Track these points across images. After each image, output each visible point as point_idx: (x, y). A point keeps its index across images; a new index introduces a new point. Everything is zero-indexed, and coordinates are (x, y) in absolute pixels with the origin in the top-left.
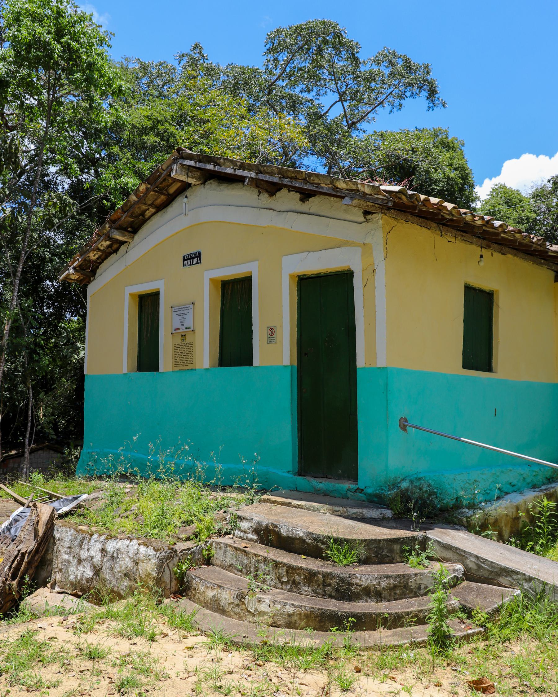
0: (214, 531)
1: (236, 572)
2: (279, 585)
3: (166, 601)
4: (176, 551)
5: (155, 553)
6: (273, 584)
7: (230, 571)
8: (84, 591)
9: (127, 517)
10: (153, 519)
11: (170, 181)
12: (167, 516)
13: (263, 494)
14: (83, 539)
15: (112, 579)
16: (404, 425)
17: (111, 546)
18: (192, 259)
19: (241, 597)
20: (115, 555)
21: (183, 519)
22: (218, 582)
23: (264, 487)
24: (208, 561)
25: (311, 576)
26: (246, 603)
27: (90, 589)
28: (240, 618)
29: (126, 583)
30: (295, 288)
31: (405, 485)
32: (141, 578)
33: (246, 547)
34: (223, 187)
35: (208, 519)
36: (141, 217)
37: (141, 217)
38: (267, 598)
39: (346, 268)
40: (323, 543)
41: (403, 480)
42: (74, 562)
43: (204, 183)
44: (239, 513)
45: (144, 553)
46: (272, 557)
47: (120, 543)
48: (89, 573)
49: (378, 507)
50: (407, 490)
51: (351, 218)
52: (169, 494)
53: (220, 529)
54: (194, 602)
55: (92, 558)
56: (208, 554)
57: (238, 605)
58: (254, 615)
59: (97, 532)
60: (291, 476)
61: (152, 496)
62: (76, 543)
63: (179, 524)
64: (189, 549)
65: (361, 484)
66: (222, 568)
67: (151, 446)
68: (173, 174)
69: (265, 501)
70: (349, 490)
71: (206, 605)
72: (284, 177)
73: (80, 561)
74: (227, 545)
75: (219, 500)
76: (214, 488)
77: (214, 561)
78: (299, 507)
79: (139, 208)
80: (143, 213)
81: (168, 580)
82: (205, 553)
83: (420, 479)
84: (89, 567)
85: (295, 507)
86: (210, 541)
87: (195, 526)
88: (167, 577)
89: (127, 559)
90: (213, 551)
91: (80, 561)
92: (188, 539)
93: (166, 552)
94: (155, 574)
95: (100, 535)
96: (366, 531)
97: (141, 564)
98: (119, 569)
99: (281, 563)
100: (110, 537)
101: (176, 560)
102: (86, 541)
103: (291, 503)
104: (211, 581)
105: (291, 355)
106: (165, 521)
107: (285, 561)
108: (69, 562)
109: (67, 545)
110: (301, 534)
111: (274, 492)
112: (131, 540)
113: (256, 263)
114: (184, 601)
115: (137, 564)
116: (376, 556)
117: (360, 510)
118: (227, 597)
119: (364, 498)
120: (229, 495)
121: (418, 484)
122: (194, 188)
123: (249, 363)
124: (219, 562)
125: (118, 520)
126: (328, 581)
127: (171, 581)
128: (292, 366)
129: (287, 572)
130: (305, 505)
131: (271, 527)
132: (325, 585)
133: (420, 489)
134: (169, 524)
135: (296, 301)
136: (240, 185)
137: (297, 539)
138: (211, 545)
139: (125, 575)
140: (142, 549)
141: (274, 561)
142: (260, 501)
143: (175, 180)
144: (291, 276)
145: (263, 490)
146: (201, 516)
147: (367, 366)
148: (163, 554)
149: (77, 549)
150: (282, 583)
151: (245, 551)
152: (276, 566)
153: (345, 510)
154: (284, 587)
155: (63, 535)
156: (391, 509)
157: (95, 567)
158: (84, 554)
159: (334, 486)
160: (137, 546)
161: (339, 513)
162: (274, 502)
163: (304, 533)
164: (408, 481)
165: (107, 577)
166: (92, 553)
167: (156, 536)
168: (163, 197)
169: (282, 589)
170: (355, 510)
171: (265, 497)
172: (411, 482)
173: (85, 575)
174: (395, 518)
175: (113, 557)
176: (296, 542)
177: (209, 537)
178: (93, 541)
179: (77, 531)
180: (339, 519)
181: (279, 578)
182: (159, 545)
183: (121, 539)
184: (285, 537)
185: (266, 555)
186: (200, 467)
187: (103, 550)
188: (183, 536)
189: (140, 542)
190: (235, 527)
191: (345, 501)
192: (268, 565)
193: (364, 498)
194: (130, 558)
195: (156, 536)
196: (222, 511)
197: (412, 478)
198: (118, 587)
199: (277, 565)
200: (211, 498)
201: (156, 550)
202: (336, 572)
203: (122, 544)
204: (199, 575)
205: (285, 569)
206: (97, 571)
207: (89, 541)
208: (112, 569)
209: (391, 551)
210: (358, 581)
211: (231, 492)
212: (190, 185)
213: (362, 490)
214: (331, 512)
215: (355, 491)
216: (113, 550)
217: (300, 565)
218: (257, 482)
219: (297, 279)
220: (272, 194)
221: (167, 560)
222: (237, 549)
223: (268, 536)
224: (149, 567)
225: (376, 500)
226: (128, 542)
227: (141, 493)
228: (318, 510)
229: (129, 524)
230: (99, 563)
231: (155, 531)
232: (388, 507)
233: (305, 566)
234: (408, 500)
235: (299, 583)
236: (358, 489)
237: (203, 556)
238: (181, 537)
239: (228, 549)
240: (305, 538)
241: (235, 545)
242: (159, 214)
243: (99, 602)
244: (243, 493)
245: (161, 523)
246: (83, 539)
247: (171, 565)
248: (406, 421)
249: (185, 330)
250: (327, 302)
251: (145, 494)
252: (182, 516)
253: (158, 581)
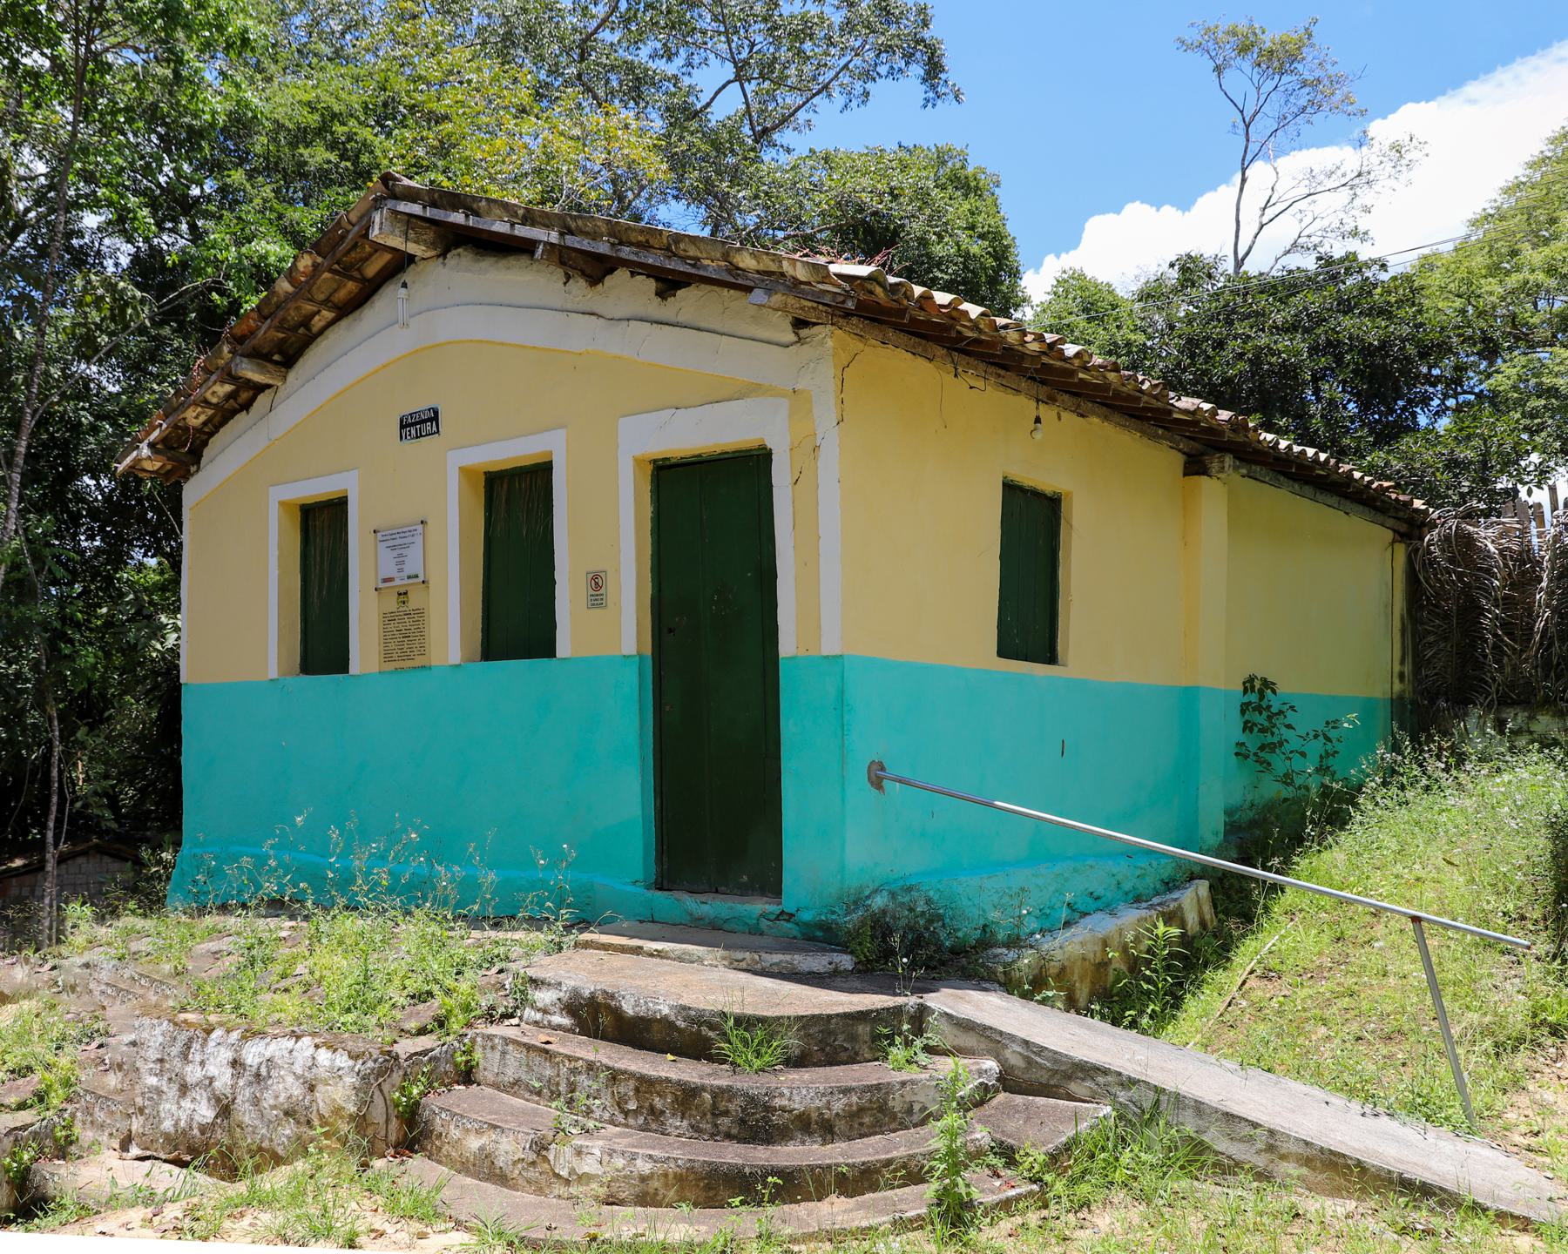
0: (478, 1012)
1: (527, 1095)
2: (620, 1118)
3: (378, 1164)
4: (397, 1058)
5: (351, 1063)
6: (607, 1116)
7: (515, 1094)
8: (194, 1151)
9: (286, 990)
10: (345, 992)
11: (368, 249)
12: (376, 985)
13: (581, 931)
14: (190, 1040)
15: (257, 1122)
16: (877, 776)
17: (253, 1054)
18: (421, 424)
19: (540, 1147)
20: (263, 1071)
21: (410, 991)
22: (489, 1118)
23: (584, 916)
24: (467, 1076)
25: (687, 1096)
26: (551, 1157)
27: (207, 1148)
28: (540, 1191)
29: (288, 1129)
30: (647, 487)
31: (879, 902)
32: (321, 1117)
33: (548, 1043)
34: (487, 263)
35: (464, 986)
36: (301, 330)
37: (301, 330)
38: (596, 1146)
39: (756, 445)
40: (712, 1027)
41: (876, 891)
42: (172, 1092)
43: (444, 255)
44: (531, 972)
45: (327, 1063)
46: (605, 1061)
47: (273, 1046)
48: (206, 1113)
49: (824, 950)
50: (884, 912)
52: (378, 938)
53: (492, 1008)
54: (439, 1162)
55: (212, 1080)
56: (467, 1062)
57: (533, 1163)
58: (568, 1182)
59: (221, 1024)
60: (642, 890)
61: (340, 943)
62: (175, 1051)
63: (402, 1001)
64: (424, 1053)
65: (788, 904)
66: (498, 1088)
67: (334, 834)
68: (374, 233)
69: (587, 945)
71: (464, 1167)
72: (621, 243)
73: (184, 1089)
74: (507, 1041)
75: (487, 947)
76: (476, 922)
77: (479, 1075)
78: (659, 954)
79: (298, 308)
80: (306, 322)
81: (382, 1120)
82: (460, 1059)
83: (910, 889)
84: (204, 1102)
85: (651, 955)
86: (471, 1033)
87: (436, 1003)
88: (378, 1113)
89: (290, 1079)
90: (477, 1055)
91: (184, 1089)
92: (422, 1031)
93: (375, 1061)
94: (352, 1109)
95: (228, 1032)
96: (800, 999)
97: (320, 1088)
98: (272, 1102)
99: (624, 1072)
100: (250, 1034)
101: (397, 1077)
102: (196, 1046)
104: (475, 1116)
105: (639, 633)
106: (371, 995)
107: (633, 1068)
108: (160, 1092)
109: (153, 1054)
110: (666, 1011)
111: (604, 925)
112: (298, 1038)
113: (562, 433)
114: (416, 1162)
115: (312, 1088)
116: (822, 1050)
117: (788, 957)
118: (509, 1149)
119: (795, 931)
120: (509, 935)
121: (906, 899)
122: (422, 265)
123: (546, 648)
124: (491, 1078)
125: (266, 997)
126: (723, 1105)
127: (387, 1121)
128: (640, 655)
129: (637, 1090)
131: (600, 999)
132: (717, 1112)
133: (911, 910)
134: (380, 1001)
135: (650, 515)
136: (524, 260)
137: (657, 1020)
138: (473, 1041)
139: (287, 1113)
140: (324, 1056)
141: (608, 1068)
142: (576, 945)
143: (379, 248)
144: (638, 462)
145: (583, 924)
146: (449, 982)
147: (802, 653)
148: (370, 1064)
149: (177, 1063)
150: (626, 1113)
151: (547, 1052)
152: (614, 1078)
154: (631, 1121)
155: (145, 1035)
156: (852, 953)
157: (218, 1100)
158: (193, 1073)
160: (312, 1049)
161: (743, 965)
162: (605, 947)
163: (671, 1007)
164: (885, 893)
165: (247, 1119)
166: (212, 1070)
167: (354, 1028)
168: (351, 286)
169: (627, 1126)
170: (776, 958)
171: (586, 936)
172: (893, 895)
173: (197, 1118)
174: (859, 972)
175: (258, 1075)
176: (656, 1027)
177: (469, 1025)
178: (211, 1044)
179: (176, 1024)
180: (743, 976)
181: (620, 1104)
182: (361, 1046)
183: (275, 1037)
184: (632, 1018)
185: (591, 1057)
186: (444, 876)
187: (235, 1063)
188: (412, 1025)
189: (317, 1040)
190: (524, 1002)
191: (757, 940)
193: (795, 931)
194: (297, 1077)
195: (354, 1028)
196: (495, 970)
197: (893, 887)
198: (271, 1140)
199: (615, 1076)
200: (470, 942)
201: (354, 1057)
202: (739, 1085)
203: (277, 1048)
204: (449, 1108)
205: (632, 1084)
206: (225, 1110)
207: (204, 1045)
208: (256, 1102)
209: (853, 1038)
210: (785, 1102)
211: (514, 929)
212: (411, 259)
213: (792, 915)
215: (777, 919)
216: (257, 1060)
217: (663, 1074)
218: (568, 906)
219: (649, 469)
220: (595, 280)
221: (379, 1075)
222: (529, 1047)
223: (595, 1016)
224: (340, 1094)
225: (823, 936)
226: (290, 1043)
227: (316, 937)
228: (700, 960)
229: (291, 1005)
230: (228, 1091)
231: (350, 1018)
232: (844, 948)
233: (674, 1076)
234: (887, 932)
235: (663, 1112)
236: (782, 912)
237: (456, 1065)
238: (407, 1026)
239: (510, 1047)
240: (673, 1018)
241: (525, 1040)
242: (344, 323)
243: (229, 1170)
244: (540, 929)
245: (362, 1000)
246: (190, 1040)
247: (386, 1087)
248: (883, 769)
249: (407, 582)
250: (714, 517)
251: (324, 940)
252: (407, 982)
253: (361, 1122)
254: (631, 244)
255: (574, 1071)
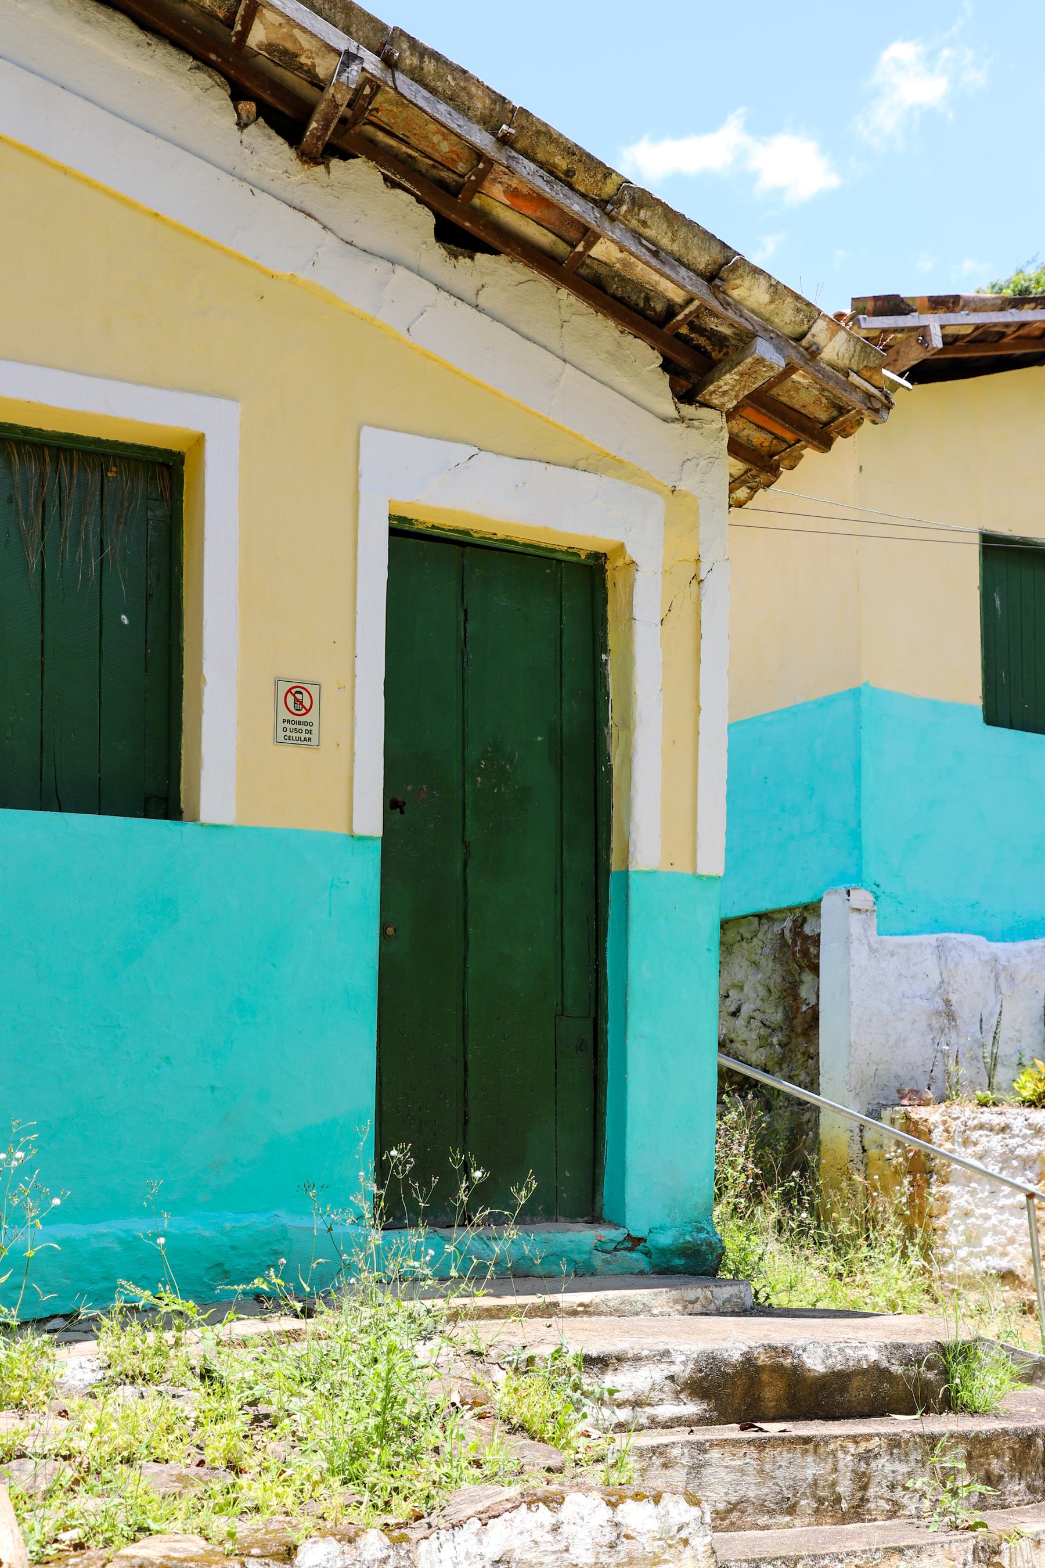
51: (631, 390)
70: (600, 1247)
103: (556, 1305)
123: (156, 788)
129: (969, 1457)
130: (605, 1302)
131: (763, 1359)
153: (709, 1294)
159: (547, 1241)
161: (698, 1307)
184: (824, 1376)
192: (905, 1458)
214: (679, 1307)
228: (647, 1309)
235: (1001, 1477)
254: (541, 165)
255: (867, 1457)
